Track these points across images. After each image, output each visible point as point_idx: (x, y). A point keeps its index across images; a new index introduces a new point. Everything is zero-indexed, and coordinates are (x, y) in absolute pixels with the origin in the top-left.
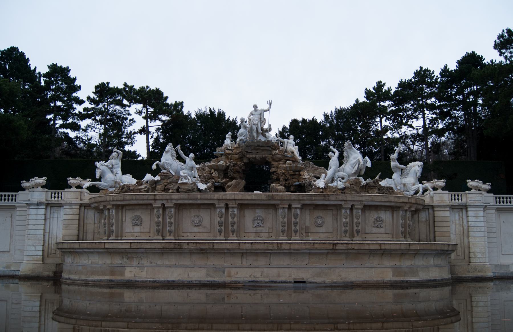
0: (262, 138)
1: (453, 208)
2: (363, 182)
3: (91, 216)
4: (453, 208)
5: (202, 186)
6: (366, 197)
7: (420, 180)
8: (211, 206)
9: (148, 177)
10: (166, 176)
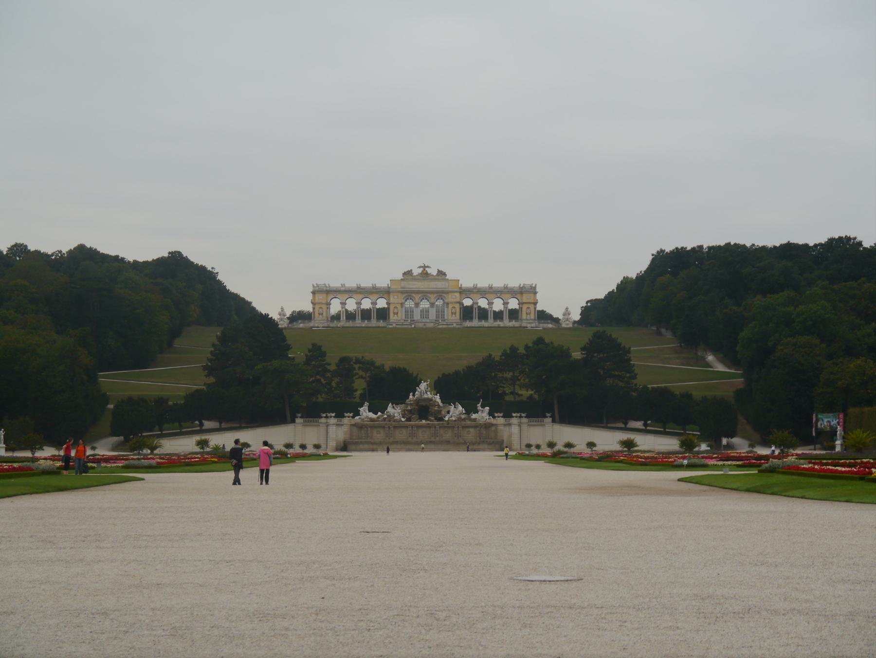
0: (426, 396)
1: (505, 425)
2: (463, 416)
3: (355, 430)
4: (505, 425)
5: (403, 419)
6: (463, 423)
7: (491, 414)
8: (406, 427)
9: (379, 413)
10: (389, 416)
